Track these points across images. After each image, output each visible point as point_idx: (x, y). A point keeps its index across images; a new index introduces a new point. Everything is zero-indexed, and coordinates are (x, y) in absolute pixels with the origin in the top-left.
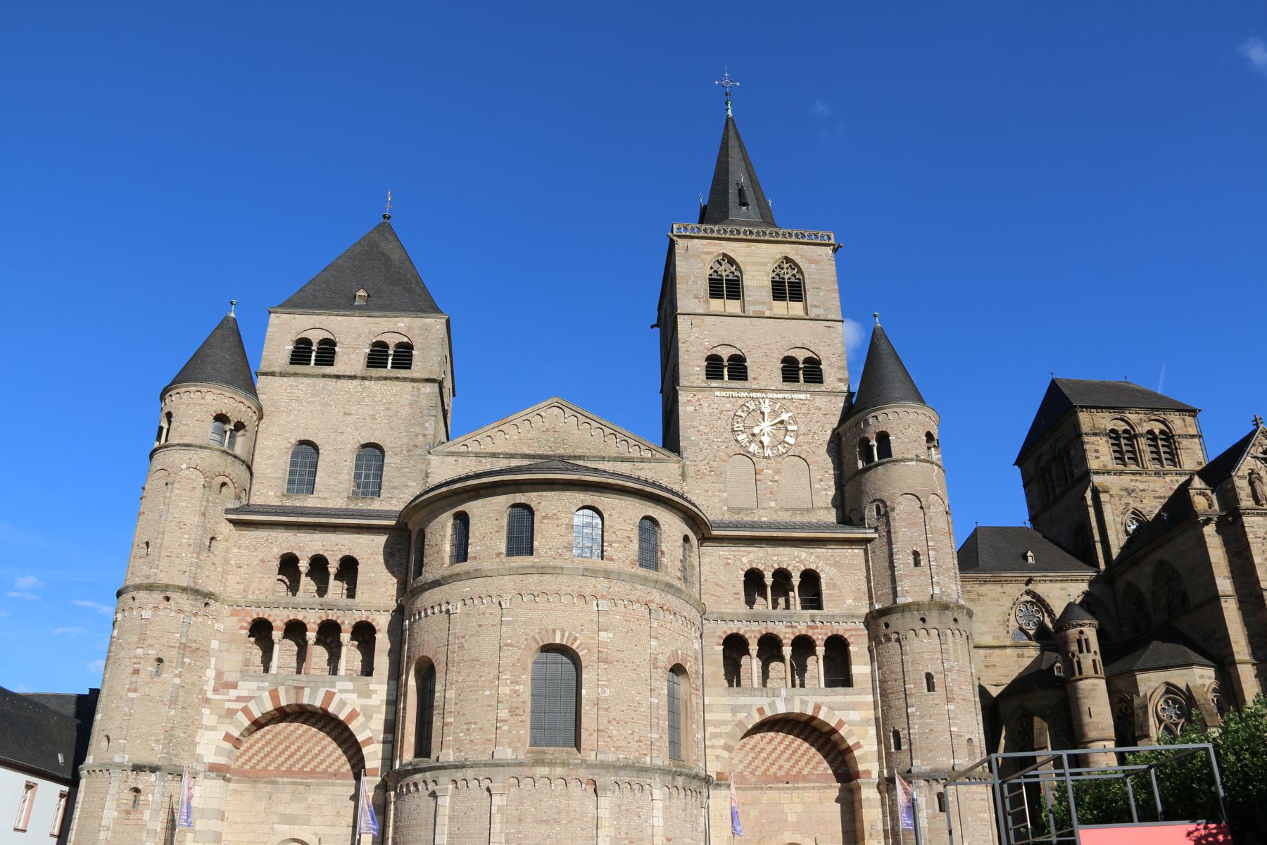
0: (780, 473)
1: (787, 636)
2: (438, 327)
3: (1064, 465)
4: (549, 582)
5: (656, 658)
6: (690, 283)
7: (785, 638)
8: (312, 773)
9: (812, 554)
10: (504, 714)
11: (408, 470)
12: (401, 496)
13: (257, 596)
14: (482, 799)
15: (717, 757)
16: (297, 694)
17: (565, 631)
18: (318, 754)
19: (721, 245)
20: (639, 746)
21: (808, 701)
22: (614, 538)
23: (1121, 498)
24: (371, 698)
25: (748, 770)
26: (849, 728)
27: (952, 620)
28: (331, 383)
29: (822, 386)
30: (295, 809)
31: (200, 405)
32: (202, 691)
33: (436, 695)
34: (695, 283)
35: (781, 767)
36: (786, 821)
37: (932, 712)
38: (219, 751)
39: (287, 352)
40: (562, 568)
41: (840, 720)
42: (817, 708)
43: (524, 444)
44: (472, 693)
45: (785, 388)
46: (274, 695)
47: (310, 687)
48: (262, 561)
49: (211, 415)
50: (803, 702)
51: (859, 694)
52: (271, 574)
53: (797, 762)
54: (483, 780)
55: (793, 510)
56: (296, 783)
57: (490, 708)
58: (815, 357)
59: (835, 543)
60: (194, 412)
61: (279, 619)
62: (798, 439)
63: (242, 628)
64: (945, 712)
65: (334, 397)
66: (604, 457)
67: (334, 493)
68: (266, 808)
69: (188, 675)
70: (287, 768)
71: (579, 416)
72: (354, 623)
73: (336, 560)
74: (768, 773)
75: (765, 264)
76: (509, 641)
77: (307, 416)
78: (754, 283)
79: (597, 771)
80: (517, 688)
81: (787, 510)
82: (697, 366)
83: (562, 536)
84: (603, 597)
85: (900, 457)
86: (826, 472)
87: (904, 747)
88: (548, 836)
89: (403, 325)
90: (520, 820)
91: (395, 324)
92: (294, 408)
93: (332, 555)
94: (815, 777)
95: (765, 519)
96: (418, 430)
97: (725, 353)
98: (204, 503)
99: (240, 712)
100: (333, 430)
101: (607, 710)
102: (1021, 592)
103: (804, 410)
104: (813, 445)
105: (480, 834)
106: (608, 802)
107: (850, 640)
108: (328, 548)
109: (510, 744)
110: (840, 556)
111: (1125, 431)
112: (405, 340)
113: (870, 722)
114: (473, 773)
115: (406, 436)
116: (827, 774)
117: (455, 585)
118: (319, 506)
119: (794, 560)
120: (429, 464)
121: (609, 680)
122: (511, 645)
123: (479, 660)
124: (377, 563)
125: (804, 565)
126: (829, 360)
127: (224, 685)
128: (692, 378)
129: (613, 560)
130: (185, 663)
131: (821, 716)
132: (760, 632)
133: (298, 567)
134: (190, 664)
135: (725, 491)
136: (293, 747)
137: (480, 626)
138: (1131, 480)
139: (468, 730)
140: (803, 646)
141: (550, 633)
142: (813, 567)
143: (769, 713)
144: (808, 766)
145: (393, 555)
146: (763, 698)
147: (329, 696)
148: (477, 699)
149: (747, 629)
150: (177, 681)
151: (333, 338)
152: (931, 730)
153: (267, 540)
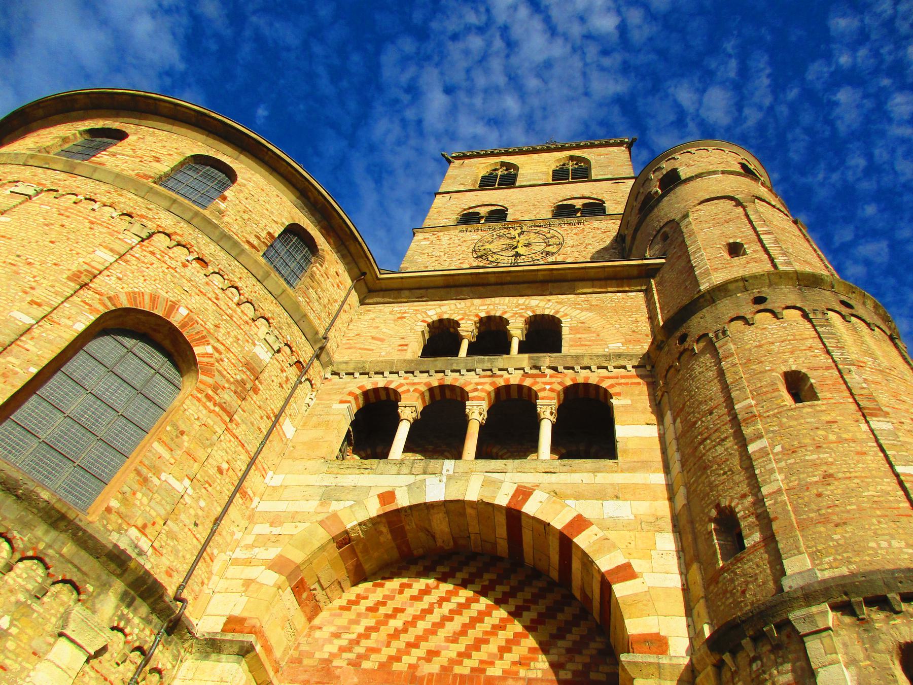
1: (479, 387)
21: (502, 482)
25: (346, 655)
26: (601, 534)
35: (432, 654)
42: (523, 493)
51: (632, 470)
53: (477, 645)
59: (590, 283)
74: (396, 666)
87: (753, 538)
113: (660, 523)
144: (506, 655)
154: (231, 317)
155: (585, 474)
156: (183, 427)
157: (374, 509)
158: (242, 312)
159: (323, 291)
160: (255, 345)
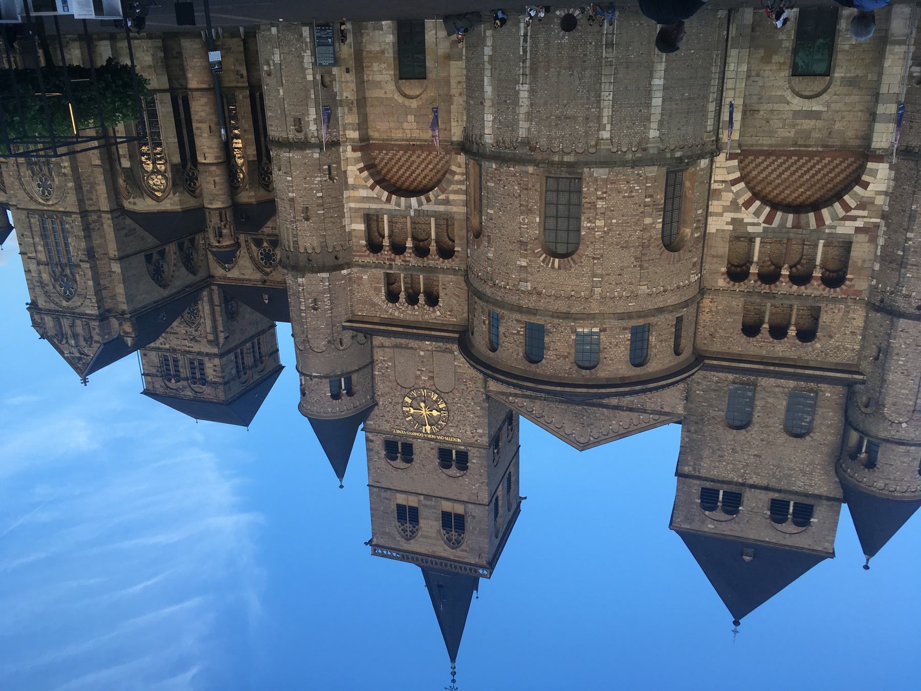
0: (416, 376)
2: (679, 520)
3: (243, 363)
4: (562, 306)
5: (489, 243)
6: (478, 529)
7: (410, 253)
8: (789, 155)
9: (391, 314)
10: (600, 204)
11: (703, 404)
12: (709, 383)
13: (835, 307)
14: (619, 136)
15: (460, 166)
16: (799, 222)
17: (551, 267)
18: (784, 171)
19: (455, 556)
20: (500, 176)
22: (515, 337)
23: (200, 336)
24: (732, 218)
27: (290, 258)
28: (773, 483)
29: (384, 438)
30: (807, 124)
31: (889, 479)
32: (887, 225)
33: (661, 220)
34: (474, 529)
35: (418, 157)
36: (415, 116)
38: (874, 173)
39: (815, 516)
40: (552, 317)
42: (388, 200)
43: (607, 416)
44: (628, 221)
45: (411, 439)
46: (820, 221)
47: (787, 228)
48: (831, 337)
49: (878, 469)
50: (398, 204)
51: (360, 209)
52: (822, 325)
53: (407, 160)
54: (617, 151)
55: (407, 347)
56: (805, 146)
57: (612, 208)
58: (389, 461)
60: (895, 473)
61: (815, 289)
62: (402, 400)
63: (851, 280)
65: (771, 472)
66: (544, 400)
67: (769, 390)
68: (834, 125)
69: (900, 240)
70: (814, 159)
71: (563, 434)
72: (746, 281)
73: (762, 334)
75: (425, 537)
76: (595, 261)
77: (795, 458)
78: (431, 523)
79: (528, 158)
80: (589, 225)
81: (412, 348)
82: (474, 463)
83: (553, 342)
84: (523, 292)
85: (324, 381)
86: (383, 374)
88: (565, 106)
89: (709, 526)
90: (587, 119)
91: (716, 527)
92: (807, 466)
93: (765, 339)
94: (395, 148)
95: (427, 343)
96: (695, 436)
97: (453, 471)
98: (883, 390)
99: (853, 206)
100: (771, 443)
101: (521, 205)
102: (272, 274)
103: (398, 421)
104: (392, 394)
105: (621, 107)
106: (520, 133)
107: (365, 249)
108: (769, 345)
109: (596, 180)
110: (371, 311)
111: (195, 383)
112: (707, 513)
114: (627, 156)
115: (705, 432)
116: (386, 150)
117: (643, 308)
118: (782, 381)
120: (685, 408)
121: (520, 228)
122: (594, 258)
123: (621, 247)
124: (725, 330)
125: (396, 306)
126: (379, 457)
127: (869, 231)
128: (477, 454)
129: (517, 320)
130: (902, 251)
131: (386, 194)
132: (428, 259)
133: (797, 330)
134: (898, 250)
135: (455, 366)
136: (807, 177)
137: (620, 275)
138: (192, 347)
139: (632, 192)
140: (398, 249)
141: (562, 266)
142: (390, 305)
143: (423, 198)
145: (711, 335)
147: (769, 220)
148: (623, 216)
149: (438, 262)
150: (909, 235)
151: (773, 523)
152: (305, 179)
153: (826, 354)
157: (431, 194)
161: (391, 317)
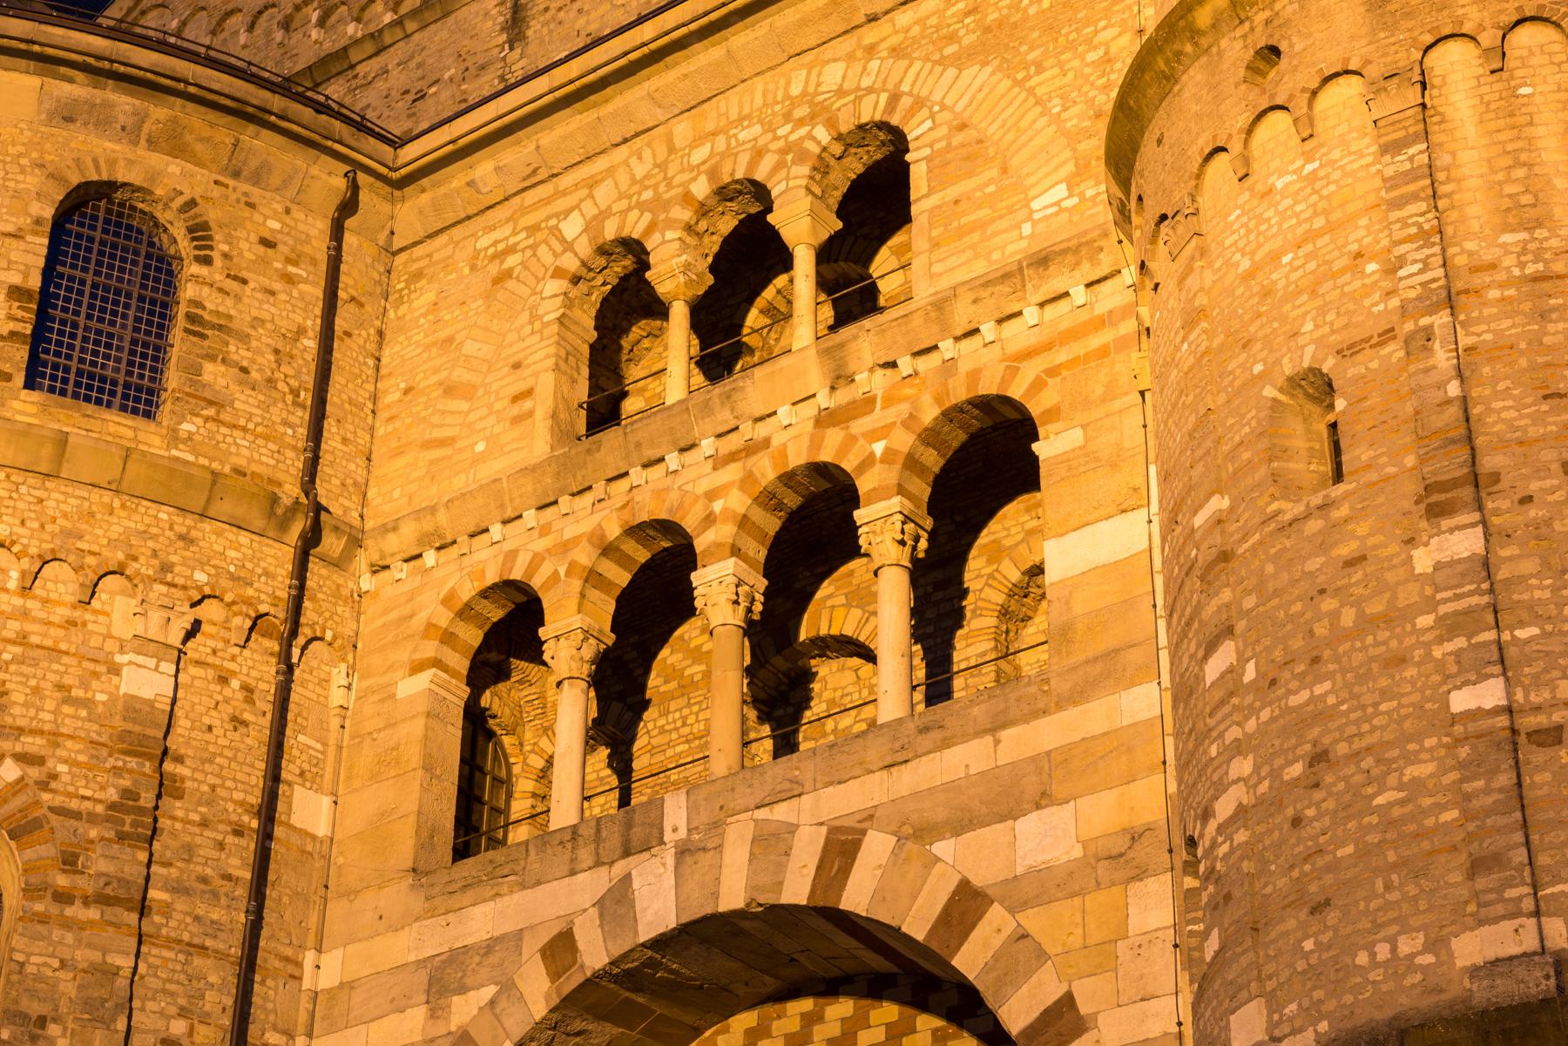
1: (717, 506)
9: (871, 50)
21: (792, 829)
26: (1009, 927)
37: (1321, 630)
41: (964, 887)
64: (1409, 595)
113: (1141, 852)
119: (787, 117)
125: (831, 123)
131: (856, 898)
143: (595, 954)
146: (581, 876)
149: (541, 545)
152: (1320, 758)
154: (22, 640)
155: (975, 743)
156: (35, 1009)
158: (45, 601)
159: (244, 338)
160: (115, 670)
161: (870, 35)
